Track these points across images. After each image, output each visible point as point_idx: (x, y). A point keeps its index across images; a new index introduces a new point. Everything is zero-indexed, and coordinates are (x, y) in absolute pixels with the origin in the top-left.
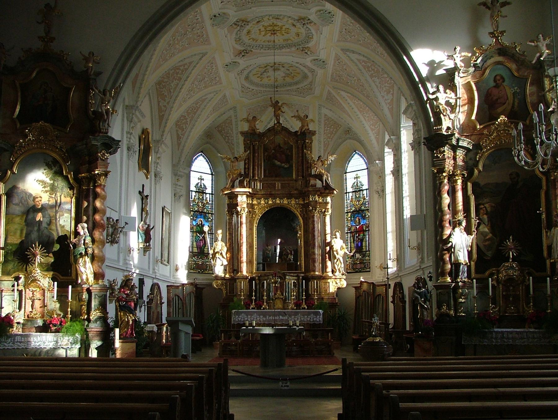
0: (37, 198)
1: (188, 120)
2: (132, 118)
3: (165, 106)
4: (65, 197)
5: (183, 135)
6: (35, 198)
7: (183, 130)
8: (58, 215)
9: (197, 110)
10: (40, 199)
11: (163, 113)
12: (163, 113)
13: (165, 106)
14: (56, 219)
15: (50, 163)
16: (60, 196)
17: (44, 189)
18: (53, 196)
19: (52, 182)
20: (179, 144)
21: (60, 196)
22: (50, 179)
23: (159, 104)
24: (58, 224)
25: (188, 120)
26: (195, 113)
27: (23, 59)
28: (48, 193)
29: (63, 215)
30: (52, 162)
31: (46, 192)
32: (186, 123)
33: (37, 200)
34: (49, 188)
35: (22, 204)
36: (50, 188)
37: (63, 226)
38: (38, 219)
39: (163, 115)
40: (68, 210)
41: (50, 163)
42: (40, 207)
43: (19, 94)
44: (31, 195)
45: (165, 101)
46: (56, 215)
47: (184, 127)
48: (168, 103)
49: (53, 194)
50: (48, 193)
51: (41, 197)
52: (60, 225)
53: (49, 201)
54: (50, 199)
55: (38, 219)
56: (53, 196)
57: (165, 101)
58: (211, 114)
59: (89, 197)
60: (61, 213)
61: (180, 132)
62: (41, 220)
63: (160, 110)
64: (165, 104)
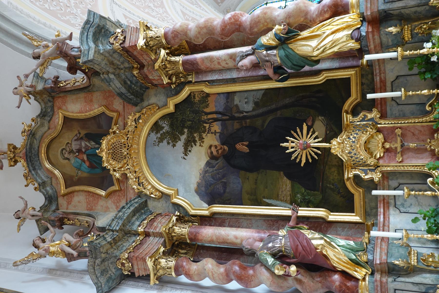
0: (212, 153)
4: (207, 106)
6: (213, 157)
8: (237, 115)
9: (195, 19)
10: (213, 149)
14: (245, 118)
15: (159, 135)
16: (207, 114)
17: (198, 144)
18: (207, 126)
19: (186, 130)
21: (207, 114)
22: (182, 133)
24: (254, 113)
27: (36, 185)
28: (204, 135)
29: (237, 106)
30: (157, 133)
31: (201, 138)
33: (215, 153)
34: (195, 135)
35: (224, 176)
36: (196, 132)
37: (256, 104)
38: (246, 149)
40: (227, 98)
41: (159, 135)
42: (226, 148)
43: (77, 188)
44: (208, 164)
46: (239, 118)
49: (205, 127)
50: (204, 135)
51: (210, 147)
52: (254, 110)
53: (215, 133)
54: (213, 130)
55: (246, 149)
56: (207, 126)
58: (200, 7)
59: (195, 59)
60: (234, 109)
62: (246, 143)
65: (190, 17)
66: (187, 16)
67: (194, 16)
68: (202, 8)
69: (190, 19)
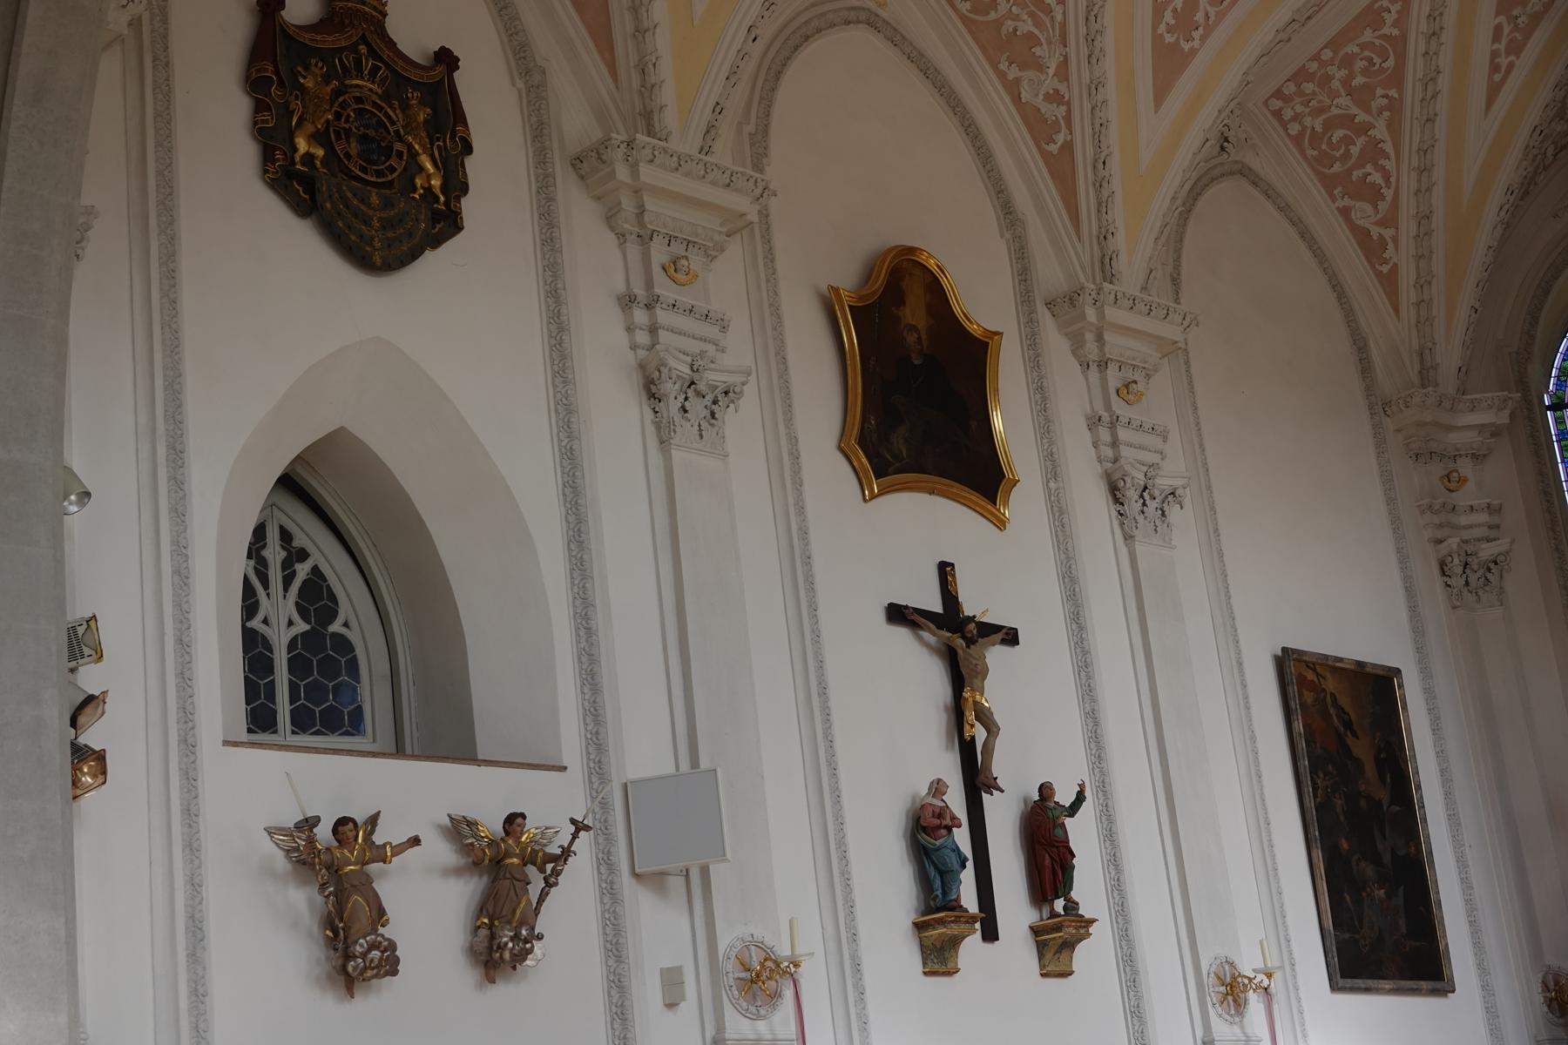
1: (1380, 131)
2: (641, 211)
3: (1055, 97)
5: (1390, 221)
7: (1373, 195)
11: (1060, 138)
12: (1060, 138)
13: (1055, 97)
20: (1389, 283)
23: (1017, 100)
25: (1380, 131)
26: (1397, 78)
32: (1374, 152)
39: (1068, 147)
45: (1041, 68)
47: (1377, 178)
48: (1063, 72)
57: (1041, 68)
58: (1516, 48)
61: (1364, 213)
63: (1039, 127)
64: (1050, 83)
65: (1396, 24)
66: (1395, 8)
67: (1416, 45)
68: (1504, 61)
69: (1386, 30)
